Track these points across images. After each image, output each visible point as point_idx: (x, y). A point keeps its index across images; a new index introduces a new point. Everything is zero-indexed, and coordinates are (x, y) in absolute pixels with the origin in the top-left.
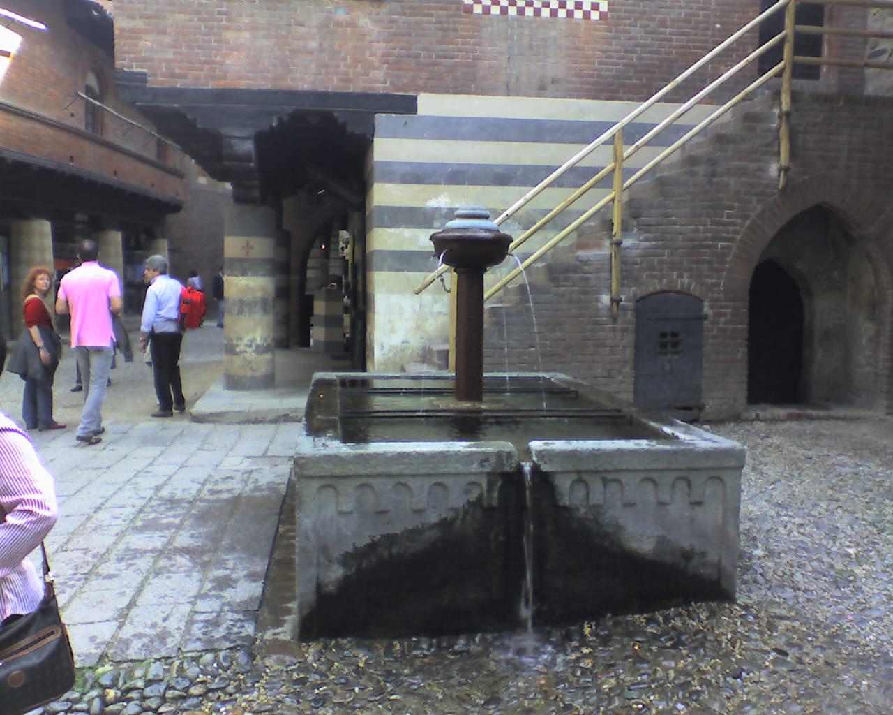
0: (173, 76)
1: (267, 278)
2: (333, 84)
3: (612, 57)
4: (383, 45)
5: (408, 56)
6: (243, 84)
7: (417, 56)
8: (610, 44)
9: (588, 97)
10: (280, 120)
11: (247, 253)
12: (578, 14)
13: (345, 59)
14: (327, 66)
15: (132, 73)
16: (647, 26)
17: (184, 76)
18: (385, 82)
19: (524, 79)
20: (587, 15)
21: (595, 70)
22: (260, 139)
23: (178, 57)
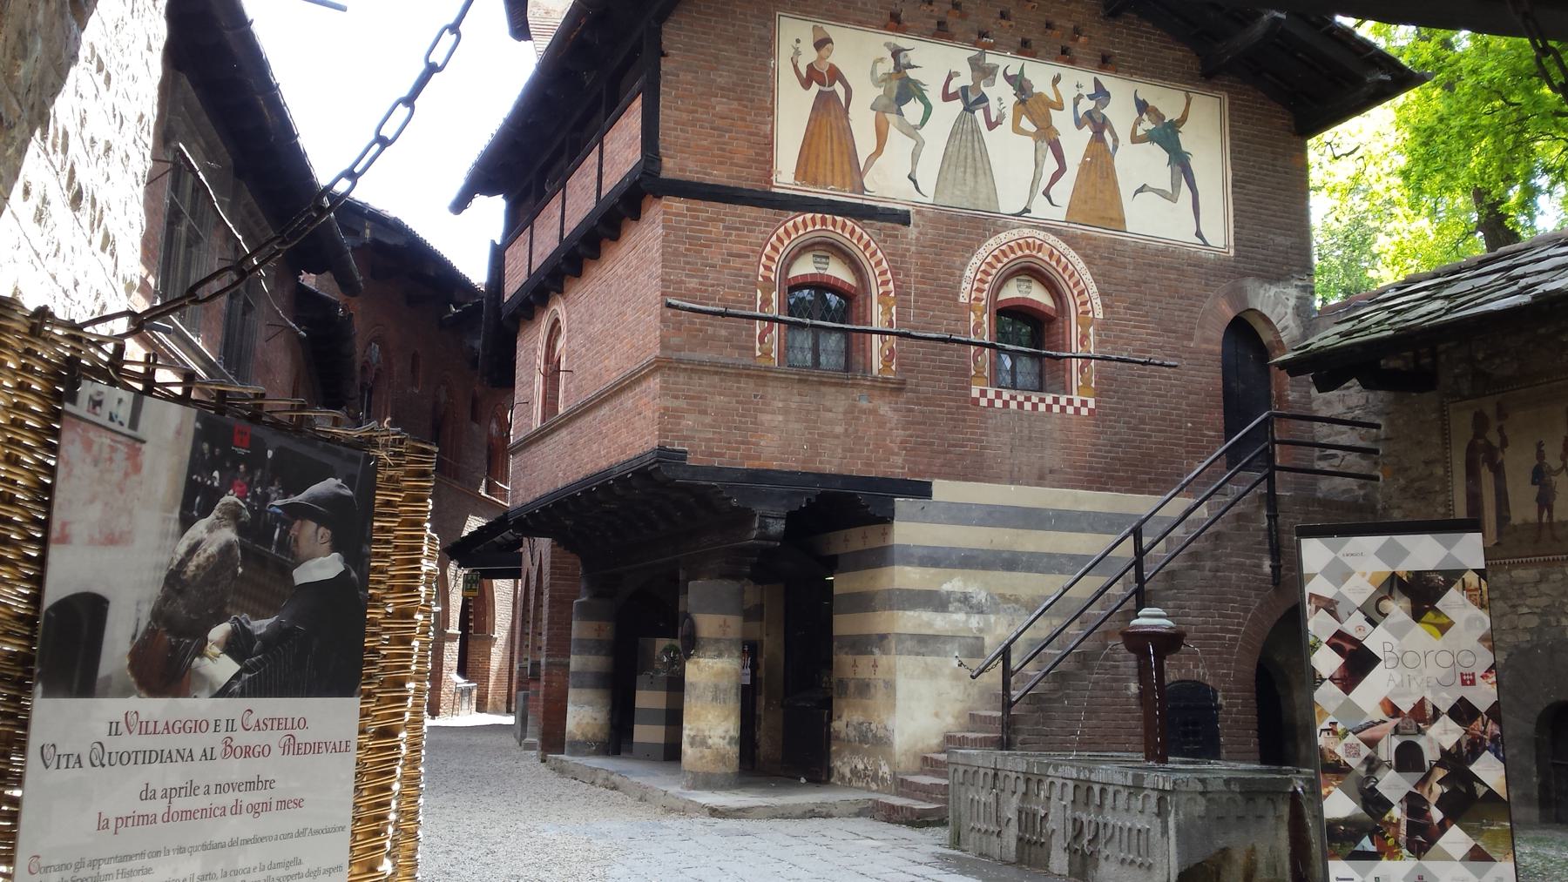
0: (711, 454)
1: (604, 658)
2: (857, 468)
3: (1100, 451)
4: (901, 432)
5: (924, 443)
6: (775, 465)
7: (932, 444)
8: (1099, 439)
9: (1083, 488)
10: (808, 500)
11: (724, 634)
12: (1070, 410)
13: (869, 444)
14: (852, 450)
15: (674, 451)
16: (1129, 423)
17: (722, 455)
18: (903, 468)
19: (1025, 468)
20: (1077, 411)
21: (1087, 462)
22: (791, 518)
23: (716, 436)
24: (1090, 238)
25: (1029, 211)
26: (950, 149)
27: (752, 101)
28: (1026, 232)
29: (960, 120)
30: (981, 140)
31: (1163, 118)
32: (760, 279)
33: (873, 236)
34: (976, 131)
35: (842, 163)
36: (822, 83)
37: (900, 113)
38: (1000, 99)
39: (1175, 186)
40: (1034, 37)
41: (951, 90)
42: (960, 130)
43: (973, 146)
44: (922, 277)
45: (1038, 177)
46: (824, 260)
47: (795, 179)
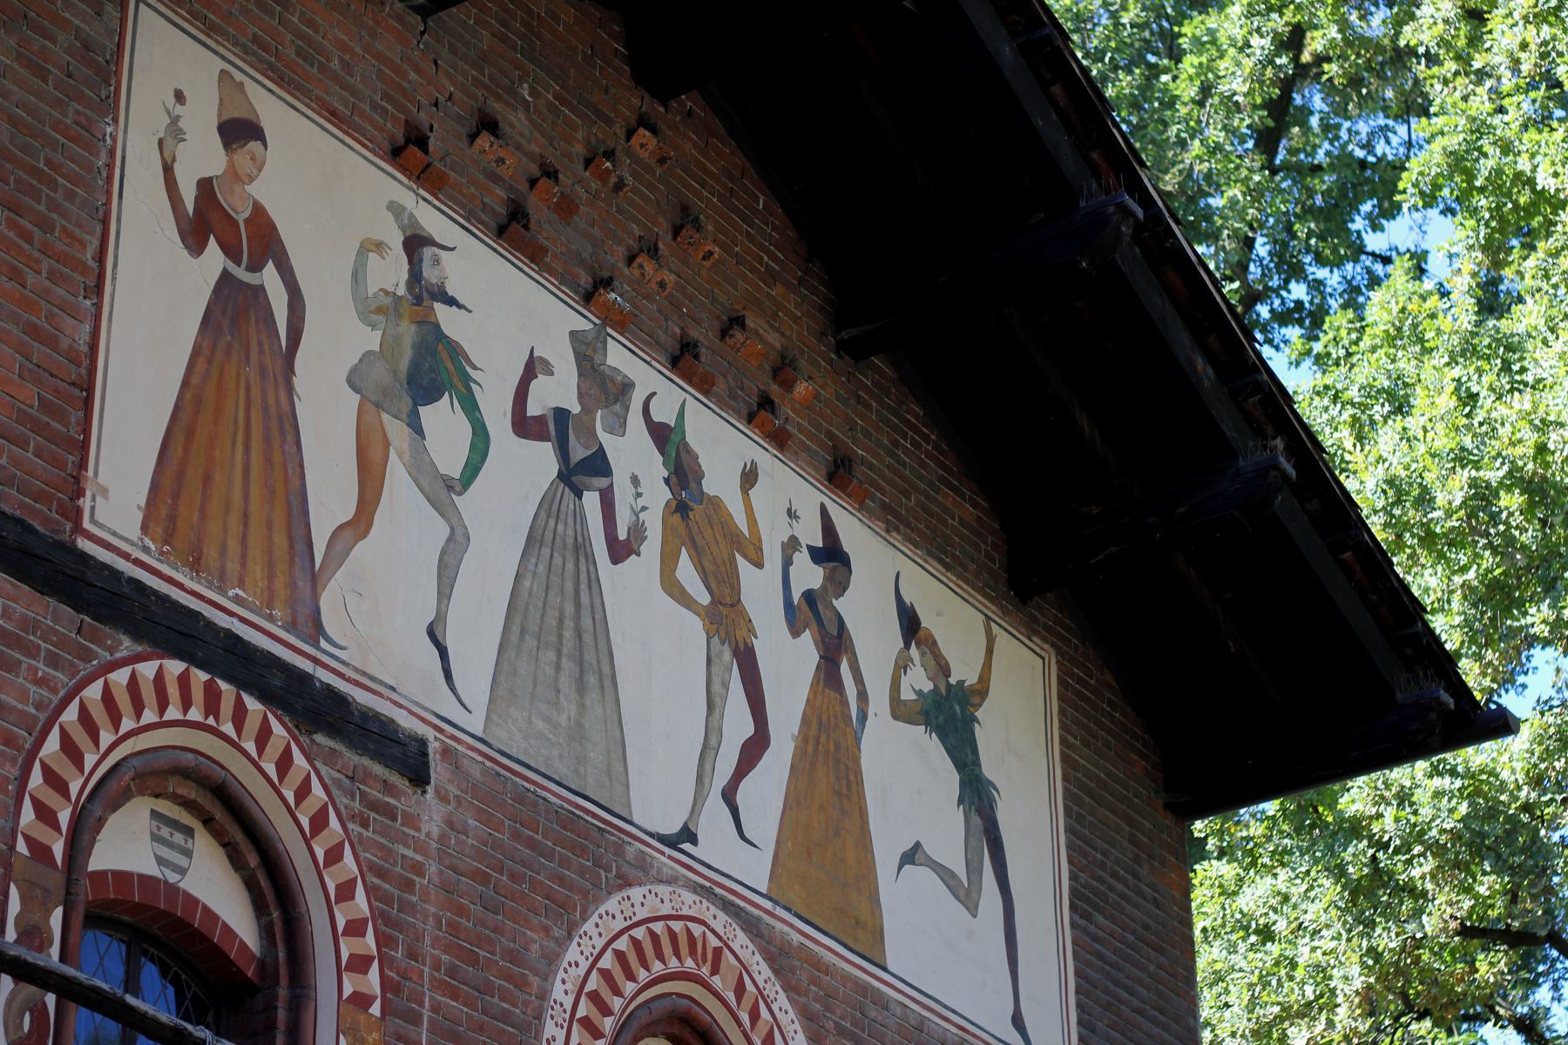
24: (817, 964)
25: (694, 841)
26: (527, 584)
27: (46, 226)
28: (689, 902)
29: (548, 505)
30: (594, 582)
31: (946, 672)
32: (22, 847)
33: (342, 800)
34: (581, 548)
35: (269, 525)
36: (232, 251)
37: (418, 430)
38: (635, 481)
39: (974, 869)
40: (704, 334)
41: (533, 409)
42: (549, 535)
43: (577, 593)
44: (452, 972)
45: (713, 741)
46: (179, 838)
47: (145, 528)
